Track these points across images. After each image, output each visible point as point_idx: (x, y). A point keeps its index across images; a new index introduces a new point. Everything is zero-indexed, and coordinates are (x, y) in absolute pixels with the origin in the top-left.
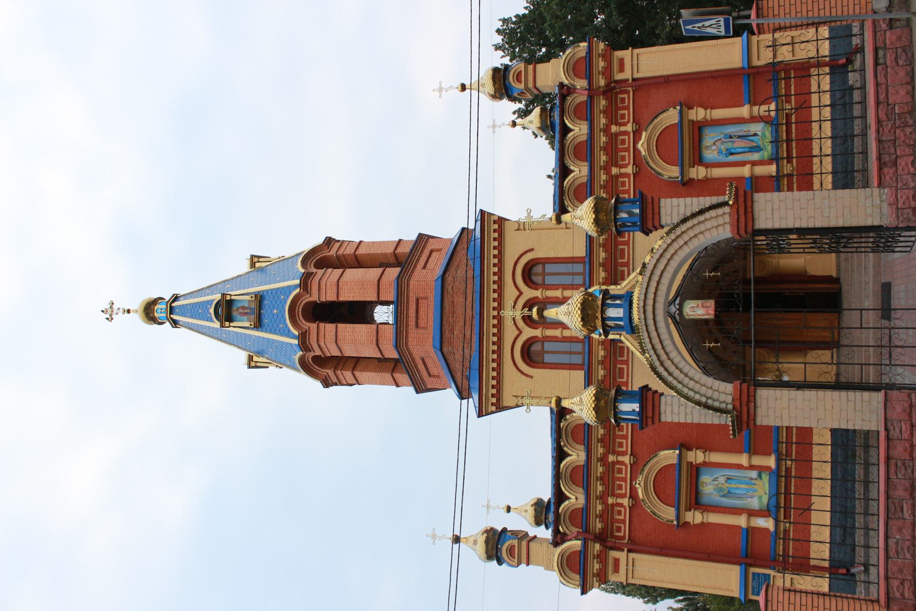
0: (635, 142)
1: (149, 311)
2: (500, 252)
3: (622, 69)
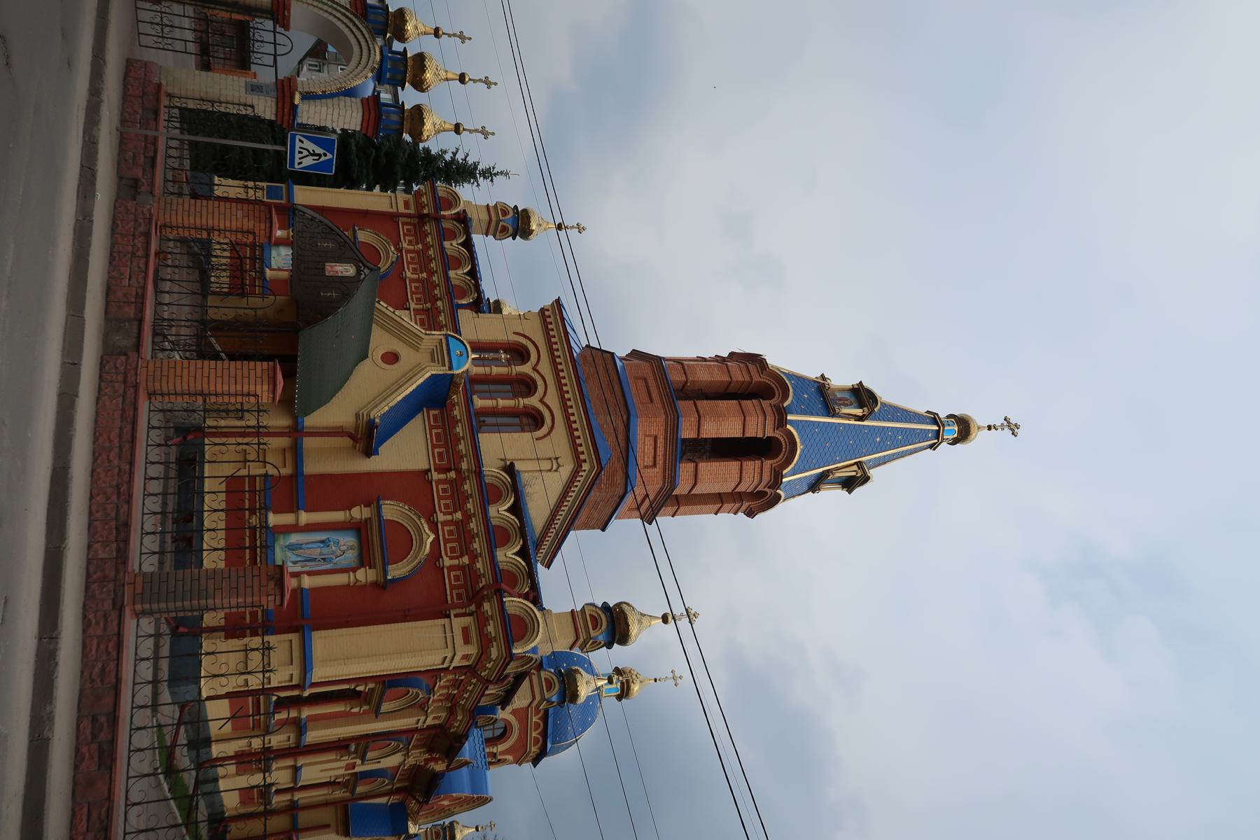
0: (437, 539)
1: (964, 429)
3: (465, 631)
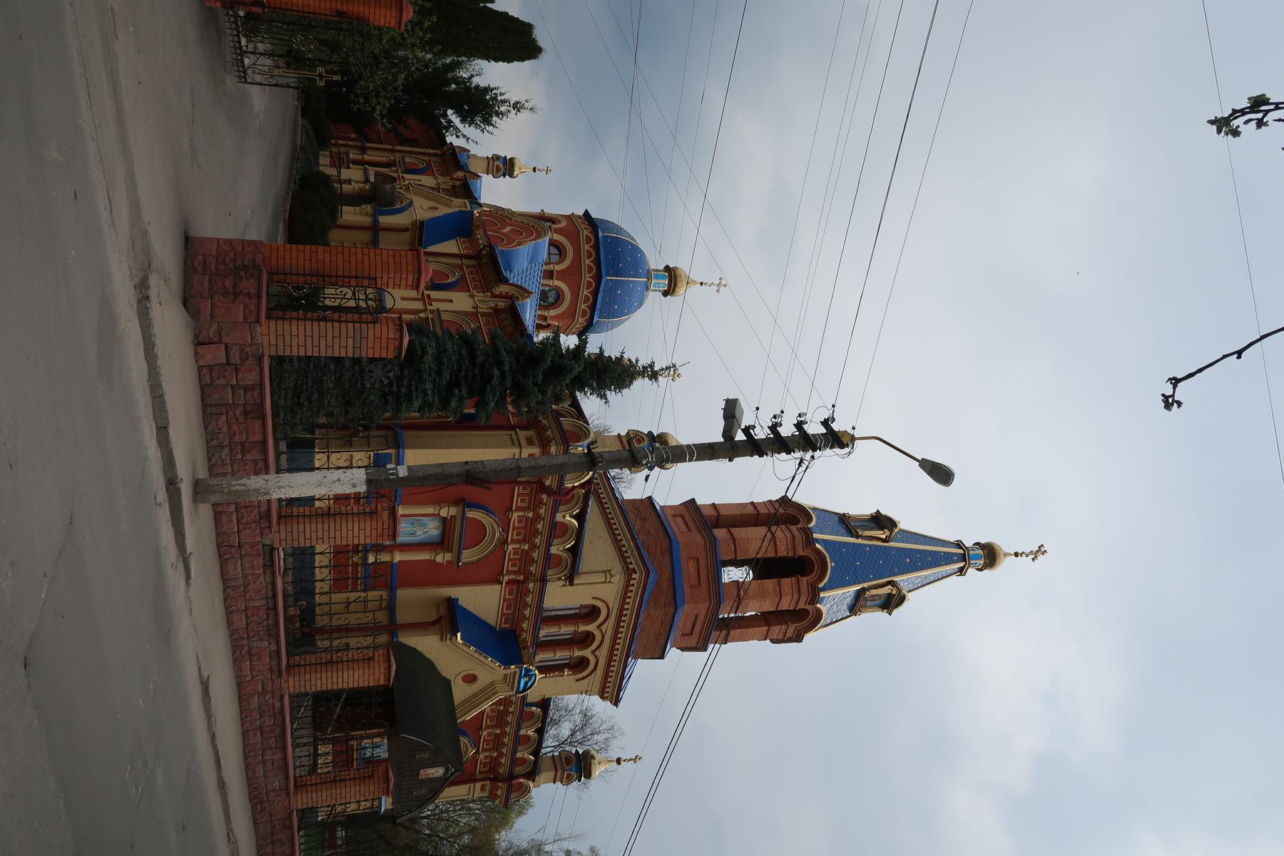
1: (990, 555)
2: (629, 581)
